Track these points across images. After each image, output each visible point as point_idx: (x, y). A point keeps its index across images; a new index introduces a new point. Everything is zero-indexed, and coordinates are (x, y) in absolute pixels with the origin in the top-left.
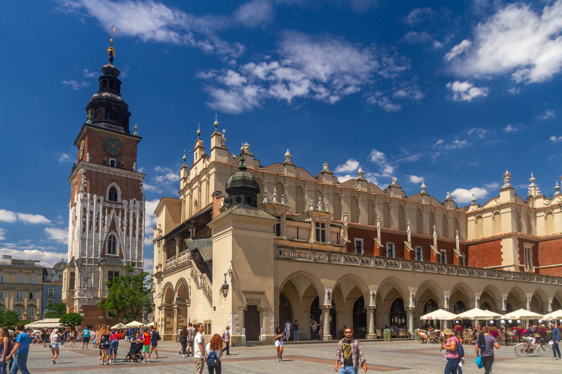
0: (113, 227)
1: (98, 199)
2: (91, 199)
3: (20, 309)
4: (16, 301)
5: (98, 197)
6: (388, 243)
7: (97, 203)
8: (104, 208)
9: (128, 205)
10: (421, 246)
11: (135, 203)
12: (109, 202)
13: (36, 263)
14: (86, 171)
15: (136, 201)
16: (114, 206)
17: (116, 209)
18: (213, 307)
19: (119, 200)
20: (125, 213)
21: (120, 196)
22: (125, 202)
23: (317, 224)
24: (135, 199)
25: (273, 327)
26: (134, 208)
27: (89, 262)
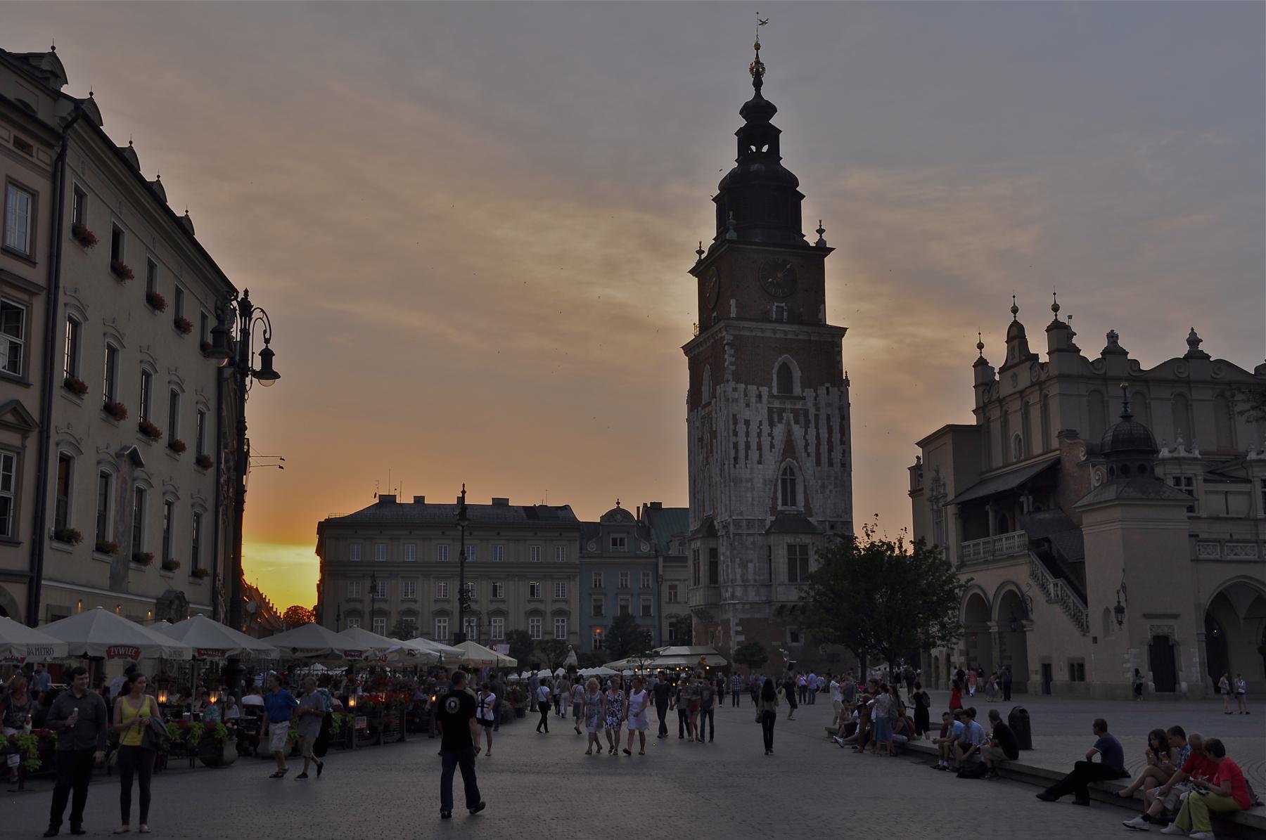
0: (789, 448)
1: (757, 393)
2: (746, 395)
3: (563, 621)
5: (758, 389)
7: (757, 402)
8: (770, 411)
9: (816, 400)
11: (828, 393)
13: (559, 512)
14: (731, 338)
15: (830, 389)
17: (793, 411)
19: (797, 390)
20: (812, 417)
22: (809, 393)
24: (828, 385)
26: (829, 405)
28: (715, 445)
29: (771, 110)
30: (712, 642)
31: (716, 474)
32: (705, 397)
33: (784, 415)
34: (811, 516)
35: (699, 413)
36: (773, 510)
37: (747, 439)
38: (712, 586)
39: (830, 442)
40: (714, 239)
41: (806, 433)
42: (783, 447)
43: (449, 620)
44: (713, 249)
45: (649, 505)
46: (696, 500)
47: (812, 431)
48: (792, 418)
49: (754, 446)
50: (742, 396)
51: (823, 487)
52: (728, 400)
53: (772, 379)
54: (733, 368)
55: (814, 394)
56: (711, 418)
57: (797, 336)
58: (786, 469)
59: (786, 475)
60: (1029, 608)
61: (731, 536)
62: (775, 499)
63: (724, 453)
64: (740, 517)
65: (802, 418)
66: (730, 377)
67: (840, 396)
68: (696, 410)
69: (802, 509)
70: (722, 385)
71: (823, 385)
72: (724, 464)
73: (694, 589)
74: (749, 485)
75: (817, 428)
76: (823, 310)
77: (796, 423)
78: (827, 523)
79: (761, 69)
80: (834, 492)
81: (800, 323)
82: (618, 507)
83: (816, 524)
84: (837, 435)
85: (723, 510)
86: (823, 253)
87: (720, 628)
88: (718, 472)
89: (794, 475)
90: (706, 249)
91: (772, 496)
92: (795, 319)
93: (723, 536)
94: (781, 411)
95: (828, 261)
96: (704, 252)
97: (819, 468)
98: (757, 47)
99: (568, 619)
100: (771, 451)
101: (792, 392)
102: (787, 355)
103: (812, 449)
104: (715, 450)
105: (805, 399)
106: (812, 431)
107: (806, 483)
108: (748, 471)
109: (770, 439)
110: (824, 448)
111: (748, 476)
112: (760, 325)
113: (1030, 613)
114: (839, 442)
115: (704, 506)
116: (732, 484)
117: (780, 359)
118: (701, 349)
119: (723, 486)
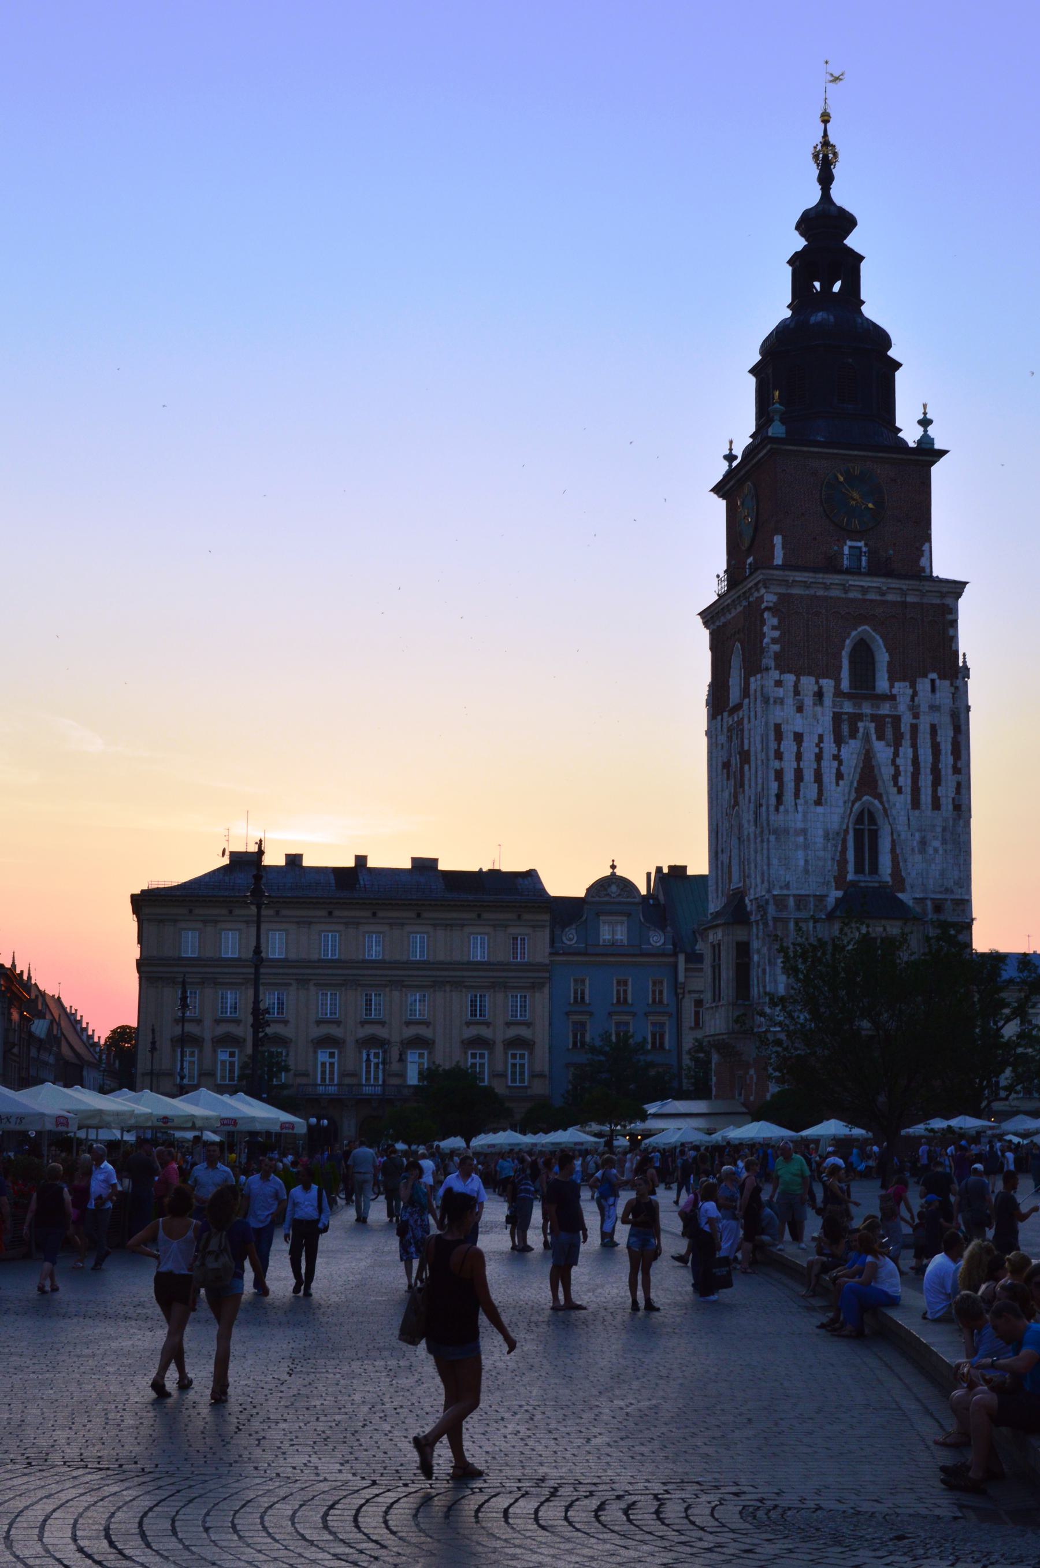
1: (816, 688)
2: (797, 692)
3: (522, 1056)
4: (468, 1024)
5: (817, 682)
7: (815, 704)
8: (837, 718)
9: (912, 699)
11: (933, 690)
12: (849, 696)
15: (938, 682)
16: (867, 709)
17: (874, 718)
19: (882, 684)
20: (905, 728)
21: (885, 669)
22: (902, 689)
24: (933, 676)
27: (798, 908)
28: (747, 774)
29: (847, 222)
30: (740, 1095)
31: (749, 821)
32: (734, 694)
33: (860, 724)
34: (903, 890)
35: (725, 721)
36: (840, 880)
37: (798, 765)
38: (740, 1002)
39: (936, 772)
40: (751, 437)
41: (896, 754)
42: (857, 777)
43: (340, 1053)
44: (749, 452)
45: (666, 870)
46: (719, 863)
47: (906, 750)
48: (873, 731)
49: (809, 775)
50: (792, 694)
51: (923, 843)
52: (766, 700)
53: (841, 667)
54: (776, 648)
55: (910, 692)
56: (742, 731)
58: (862, 813)
59: (862, 823)
61: (771, 923)
62: (842, 863)
63: (760, 787)
64: (785, 892)
65: (889, 732)
66: (772, 664)
67: (953, 694)
68: (719, 718)
69: (889, 879)
70: (759, 676)
71: (926, 676)
72: (761, 805)
73: (712, 1008)
74: (801, 839)
75: (914, 746)
76: (927, 554)
77: (881, 737)
78: (929, 903)
79: (831, 156)
80: (941, 852)
81: (889, 574)
82: (613, 874)
83: (911, 903)
84: (947, 760)
85: (759, 880)
86: (931, 459)
87: (752, 1072)
88: (752, 817)
89: (875, 824)
90: (738, 451)
91: (837, 858)
92: (879, 567)
93: (757, 922)
94: (855, 719)
95: (938, 472)
96: (736, 457)
97: (917, 812)
98: (826, 118)
99: (201, 1052)
100: (838, 784)
101: (874, 688)
102: (867, 627)
103: (905, 781)
104: (746, 782)
106: (906, 750)
107: (895, 837)
108: (800, 816)
109: (835, 764)
110: (926, 780)
111: (800, 825)
112: (820, 577)
114: (950, 771)
115: (730, 873)
116: (772, 838)
117: (854, 633)
118: (729, 617)
119: (759, 840)
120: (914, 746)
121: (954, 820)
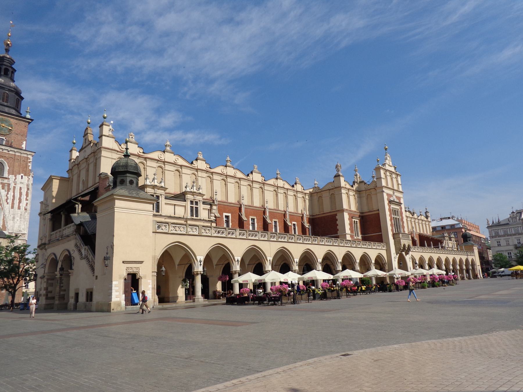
6: (251, 217)
9: (15, 180)
10: (277, 219)
11: (22, 178)
15: (23, 177)
18: (95, 277)
20: (12, 187)
22: (12, 177)
23: (192, 202)
24: (23, 175)
25: (151, 292)
41: (8, 194)
47: (11, 193)
51: (14, 218)
55: (15, 178)
57: (9, 152)
60: (73, 263)
65: (6, 188)
71: (20, 174)
75: (14, 192)
80: (19, 220)
81: (11, 146)
97: (13, 210)
102: (2, 159)
105: (9, 179)
107: (4, 216)
110: (17, 201)
113: (73, 265)
120: (14, 192)
121: (24, 212)
